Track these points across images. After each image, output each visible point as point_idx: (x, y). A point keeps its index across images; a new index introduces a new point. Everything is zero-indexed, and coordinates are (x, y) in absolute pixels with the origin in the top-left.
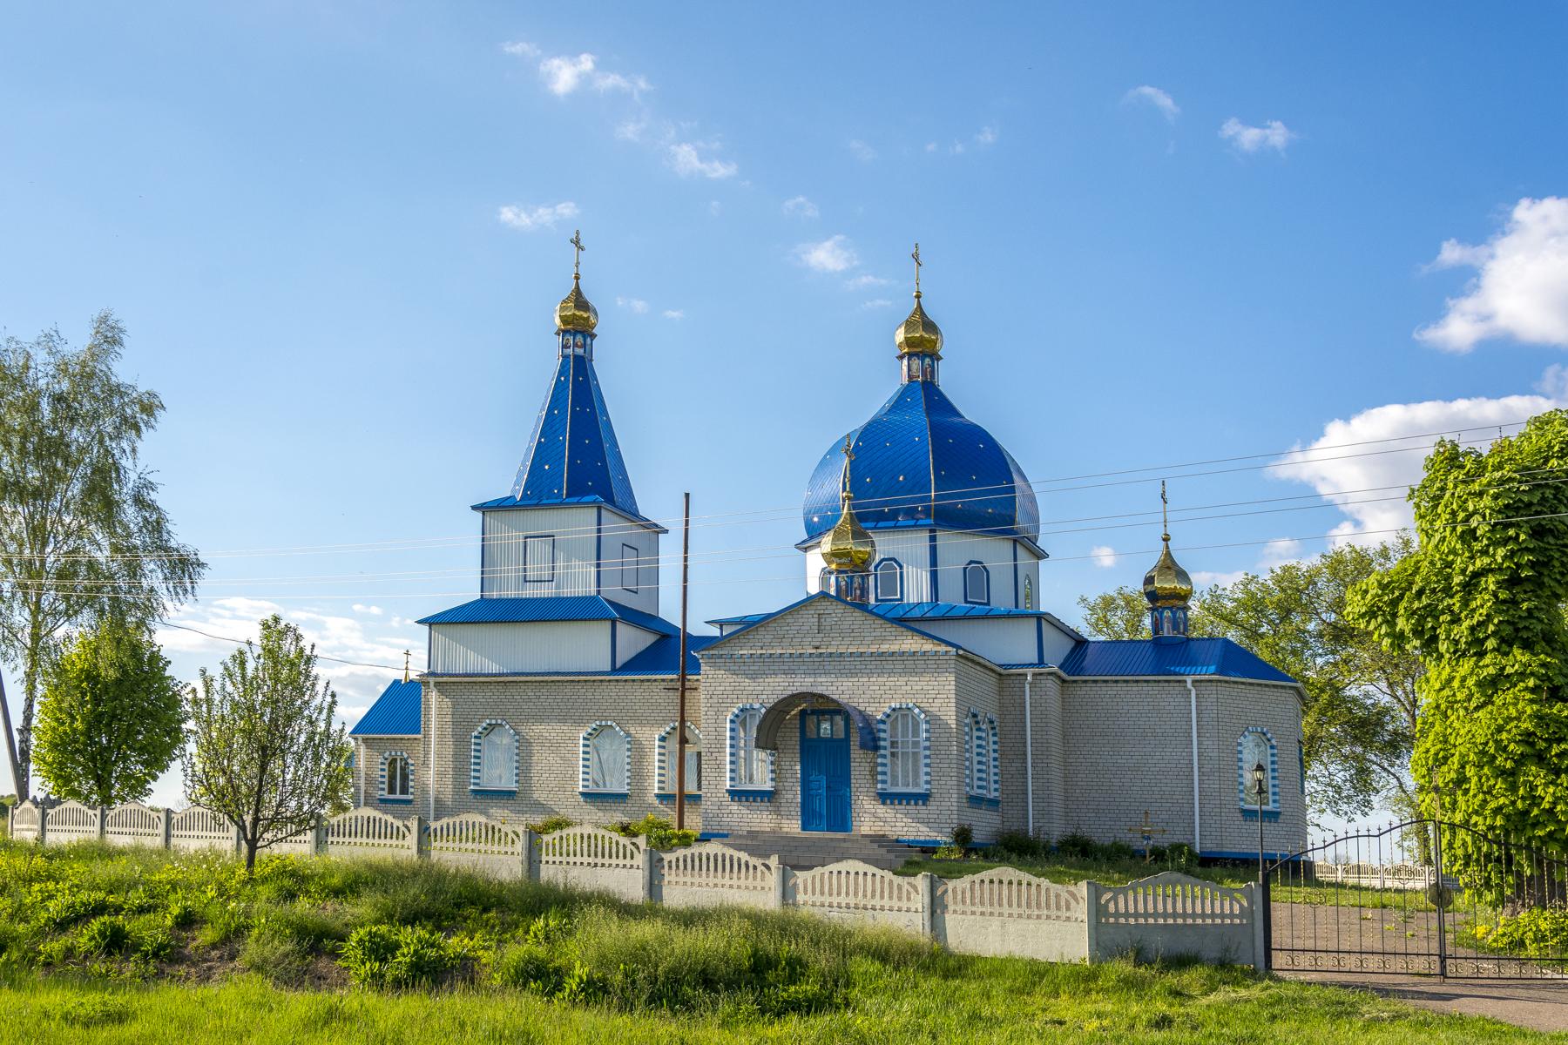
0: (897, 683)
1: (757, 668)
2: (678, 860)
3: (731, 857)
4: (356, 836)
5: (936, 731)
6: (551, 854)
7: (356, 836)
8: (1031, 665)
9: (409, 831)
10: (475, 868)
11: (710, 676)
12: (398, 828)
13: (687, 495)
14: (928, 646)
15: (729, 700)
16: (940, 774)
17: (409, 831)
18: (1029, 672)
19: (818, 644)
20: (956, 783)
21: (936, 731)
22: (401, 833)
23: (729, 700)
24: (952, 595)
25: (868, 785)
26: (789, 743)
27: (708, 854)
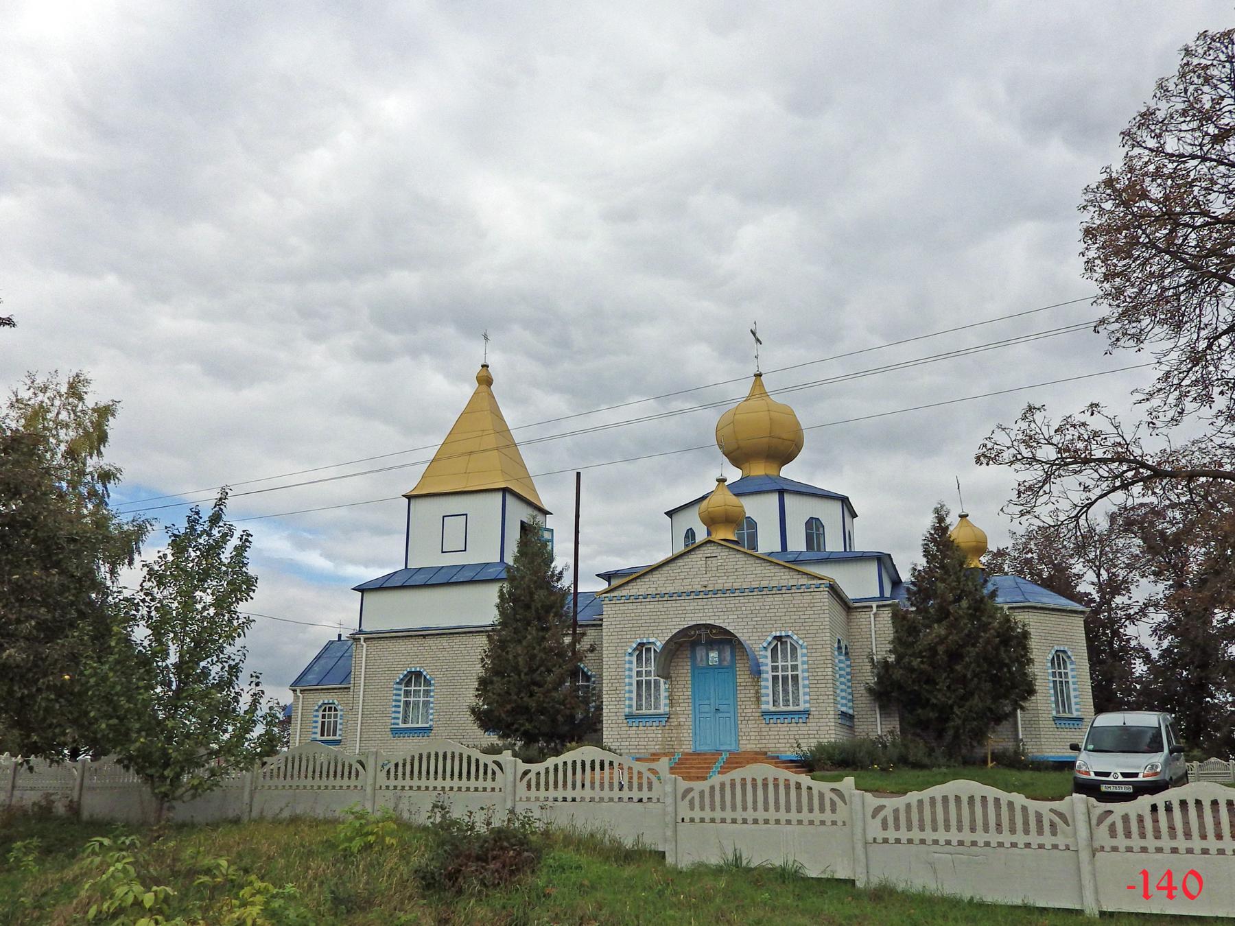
0: (777, 614)
1: (652, 606)
2: (712, 788)
3: (997, 800)
4: (469, 778)
5: (813, 655)
6: (954, 829)
7: (469, 778)
8: (873, 599)
9: (501, 769)
10: (923, 891)
11: (611, 616)
12: (486, 765)
13: (578, 474)
14: (804, 581)
15: (628, 636)
16: (818, 693)
17: (501, 769)
18: (874, 605)
19: (706, 583)
20: (832, 701)
21: (813, 655)
22: (490, 772)
23: (628, 636)
24: (798, 543)
25: (753, 707)
26: (681, 671)
27: (754, 780)
